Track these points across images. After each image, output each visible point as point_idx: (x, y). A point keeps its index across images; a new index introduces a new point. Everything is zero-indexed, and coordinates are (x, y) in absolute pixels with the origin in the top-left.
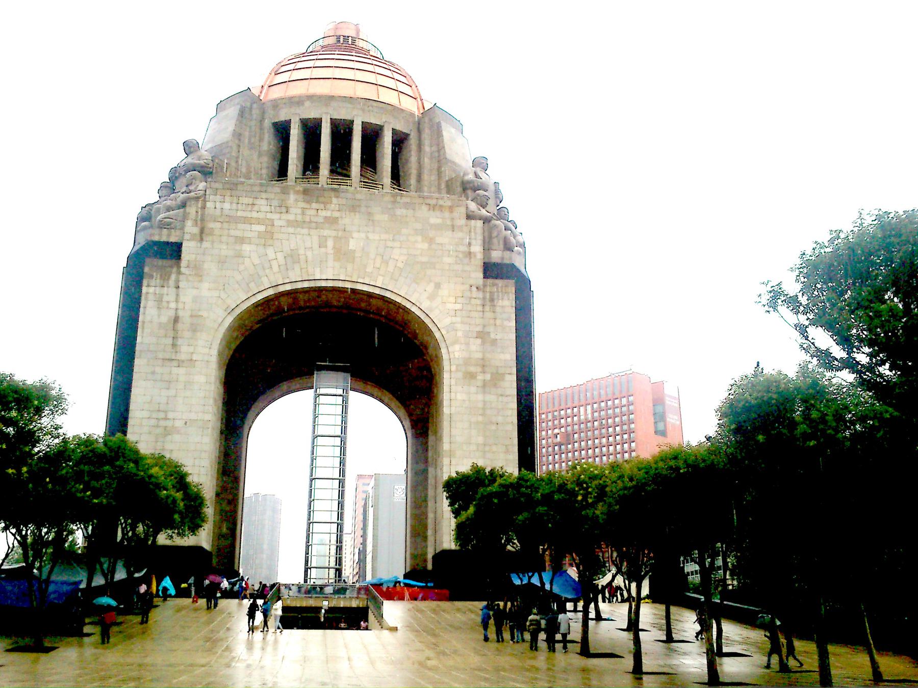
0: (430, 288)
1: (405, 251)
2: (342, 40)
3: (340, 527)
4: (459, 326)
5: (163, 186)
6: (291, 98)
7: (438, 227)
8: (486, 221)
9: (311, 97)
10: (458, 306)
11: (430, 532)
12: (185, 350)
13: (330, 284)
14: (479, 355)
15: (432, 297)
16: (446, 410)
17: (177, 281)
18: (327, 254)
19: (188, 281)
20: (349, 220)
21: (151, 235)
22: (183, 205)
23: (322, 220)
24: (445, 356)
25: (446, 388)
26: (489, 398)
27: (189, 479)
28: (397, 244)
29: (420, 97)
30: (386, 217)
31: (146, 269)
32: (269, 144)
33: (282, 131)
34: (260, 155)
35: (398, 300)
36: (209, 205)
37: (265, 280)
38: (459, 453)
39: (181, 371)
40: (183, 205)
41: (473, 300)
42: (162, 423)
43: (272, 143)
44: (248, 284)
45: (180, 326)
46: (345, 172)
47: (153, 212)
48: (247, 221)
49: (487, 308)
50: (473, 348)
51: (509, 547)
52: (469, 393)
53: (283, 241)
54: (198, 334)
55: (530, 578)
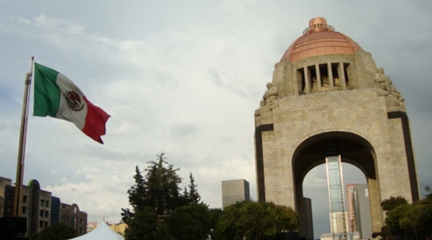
0: (367, 126)
5: (261, 102)
8: (386, 95)
10: (379, 132)
14: (390, 150)
15: (368, 130)
25: (379, 165)
30: (345, 101)
31: (263, 136)
33: (301, 71)
39: (280, 171)
41: (385, 129)
46: (327, 82)
50: (388, 147)
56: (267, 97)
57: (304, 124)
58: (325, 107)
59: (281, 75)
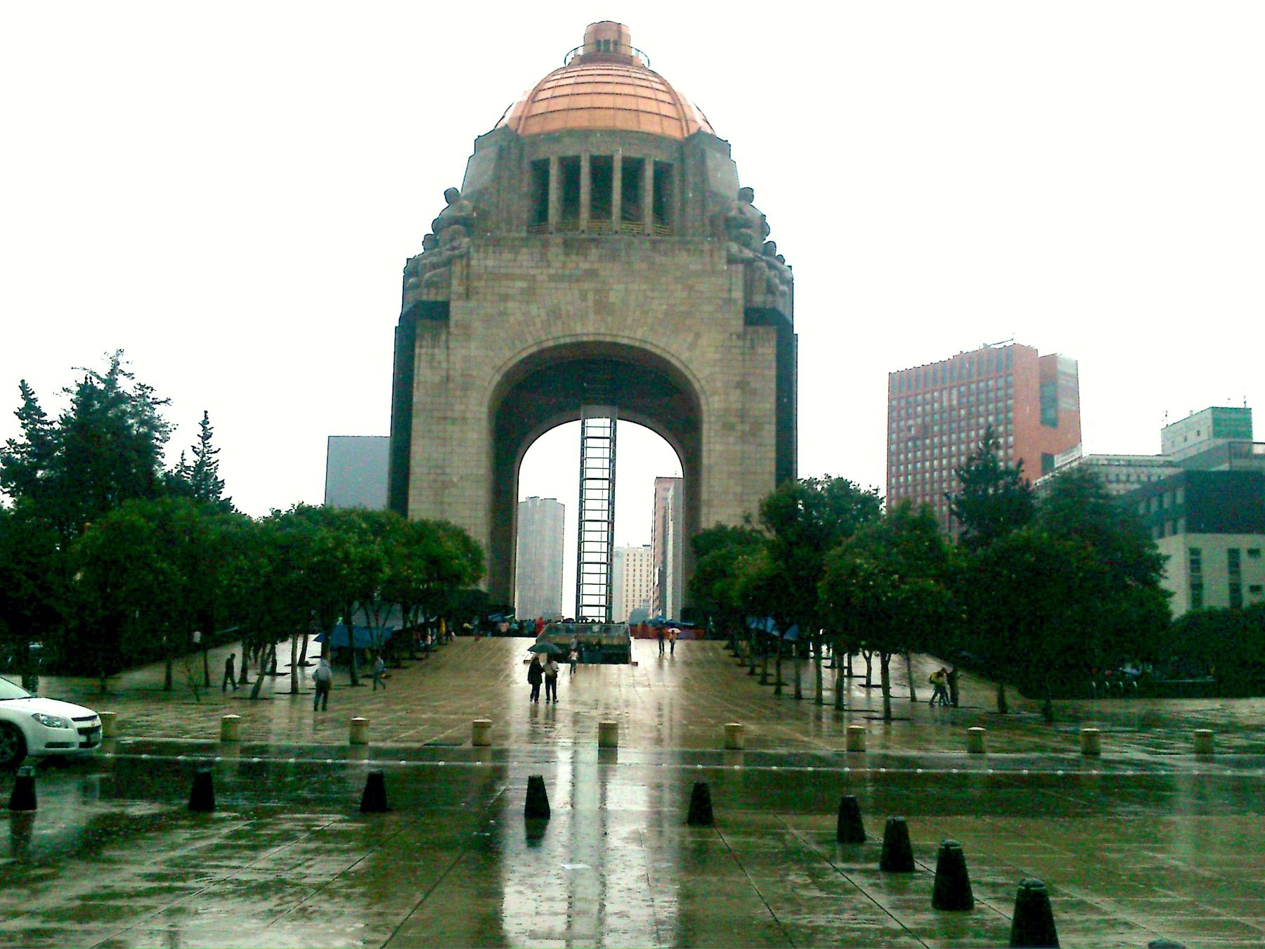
9: (571, 133)
10: (718, 356)
13: (591, 338)
15: (692, 347)
16: (705, 461)
17: (447, 341)
18: (587, 307)
19: (457, 341)
20: (609, 271)
22: (449, 262)
24: (704, 408)
25: (705, 440)
28: (656, 294)
30: (644, 266)
31: (418, 331)
33: (541, 169)
35: (658, 352)
36: (474, 263)
37: (528, 336)
38: (716, 502)
40: (449, 262)
41: (734, 350)
42: (440, 478)
47: (419, 268)
48: (508, 277)
52: (727, 444)
54: (469, 393)
56: (444, 227)
58: (592, 274)
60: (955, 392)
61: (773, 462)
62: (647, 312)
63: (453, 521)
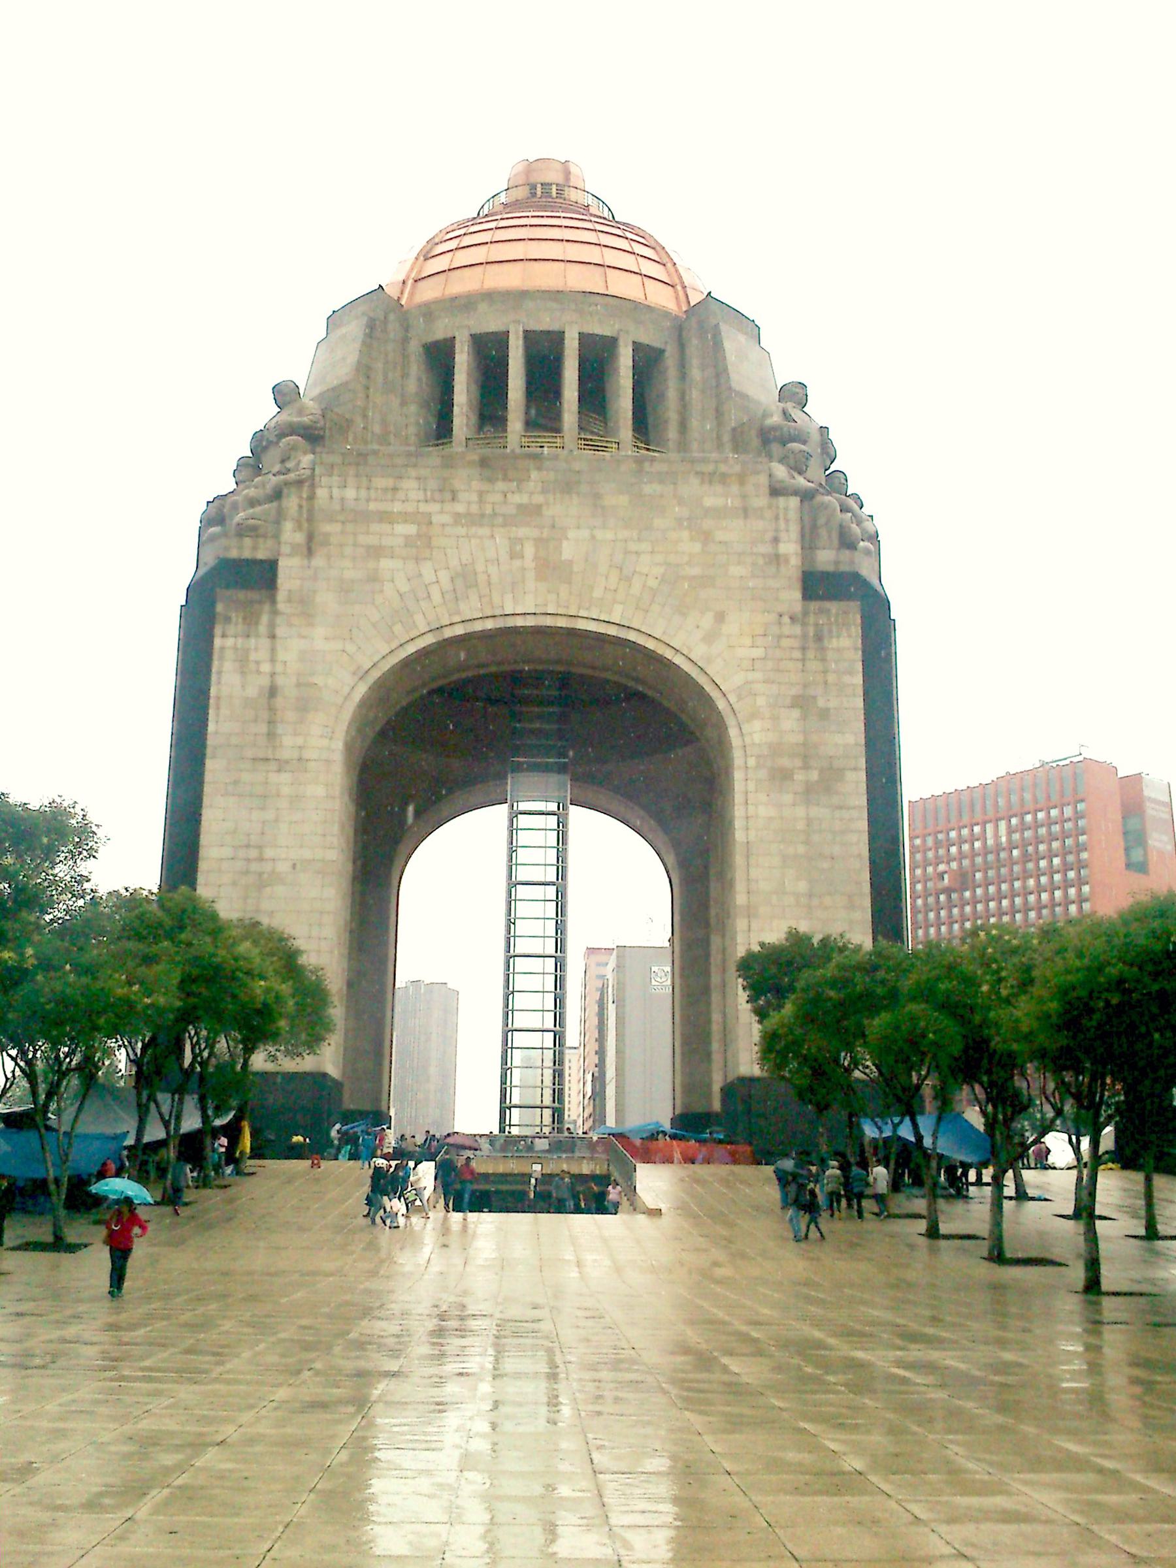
0: (707, 621)
1: (659, 558)
2: (539, 193)
3: (559, 1038)
4: (760, 687)
5: (242, 463)
6: (454, 299)
7: (719, 513)
8: (806, 496)
9: (490, 296)
10: (758, 653)
11: (715, 1046)
12: (288, 742)
13: (530, 622)
15: (710, 638)
16: (739, 835)
17: (272, 625)
18: (524, 569)
19: (290, 625)
21: (227, 549)
22: (277, 495)
23: (514, 511)
25: (738, 798)
26: (815, 811)
27: (303, 960)
28: (645, 546)
29: (682, 283)
30: (623, 500)
31: (219, 608)
32: (419, 379)
34: (403, 403)
35: (650, 645)
36: (321, 493)
39: (285, 777)
40: (277, 495)
42: (254, 867)
43: (424, 380)
44: (390, 627)
45: (279, 701)
48: (385, 517)
49: (810, 654)
51: (857, 1074)
53: (449, 551)
55: (895, 1127)
57: (421, 575)
59: (350, 354)
60: (1003, 825)
61: (865, 837)
62: (629, 579)
63: (265, 921)
